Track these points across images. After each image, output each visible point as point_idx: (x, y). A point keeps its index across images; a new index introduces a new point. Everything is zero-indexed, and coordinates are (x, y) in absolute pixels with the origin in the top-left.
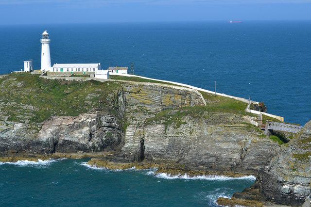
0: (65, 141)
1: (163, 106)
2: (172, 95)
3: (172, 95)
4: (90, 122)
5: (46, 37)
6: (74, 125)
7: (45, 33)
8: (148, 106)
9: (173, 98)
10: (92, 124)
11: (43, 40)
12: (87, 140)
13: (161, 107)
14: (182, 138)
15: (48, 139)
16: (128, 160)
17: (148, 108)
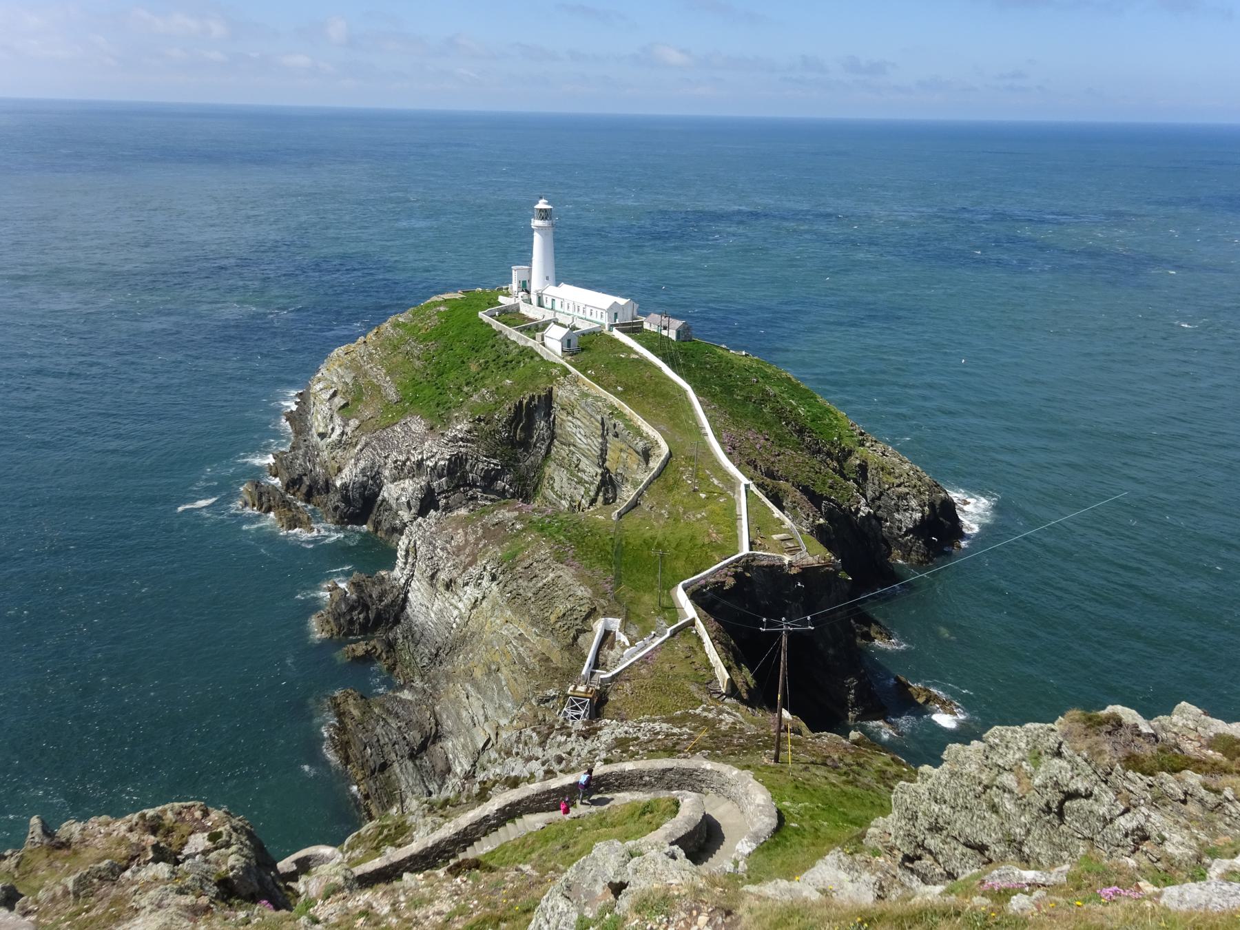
0: (384, 500)
1: (608, 471)
2: (624, 446)
3: (624, 446)
4: (434, 468)
5: (545, 215)
6: (404, 463)
7: (542, 204)
8: (583, 459)
9: (624, 455)
10: (437, 472)
11: (536, 223)
12: (413, 511)
13: (600, 471)
14: (456, 613)
15: (345, 486)
16: (351, 622)
17: (585, 464)
